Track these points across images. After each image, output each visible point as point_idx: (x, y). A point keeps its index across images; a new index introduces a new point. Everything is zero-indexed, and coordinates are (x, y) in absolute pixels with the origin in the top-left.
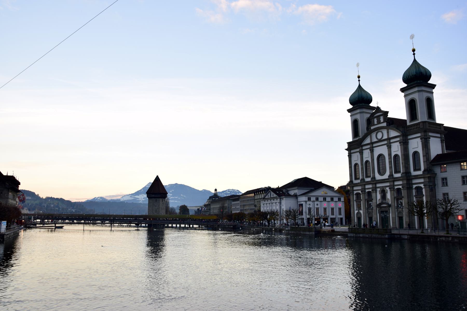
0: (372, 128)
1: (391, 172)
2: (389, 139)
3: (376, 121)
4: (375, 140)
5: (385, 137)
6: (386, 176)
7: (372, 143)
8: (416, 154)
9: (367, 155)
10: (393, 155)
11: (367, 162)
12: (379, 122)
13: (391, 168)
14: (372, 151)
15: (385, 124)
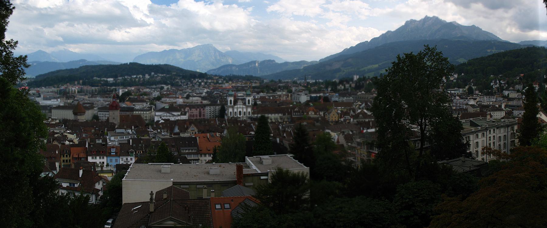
0: (238, 104)
1: (243, 115)
2: (243, 108)
3: (239, 102)
4: (238, 107)
5: (242, 107)
6: (242, 116)
7: (237, 108)
8: (249, 112)
9: (235, 110)
10: (244, 111)
11: (236, 112)
12: (240, 103)
13: (243, 114)
14: (237, 110)
15: (242, 104)
